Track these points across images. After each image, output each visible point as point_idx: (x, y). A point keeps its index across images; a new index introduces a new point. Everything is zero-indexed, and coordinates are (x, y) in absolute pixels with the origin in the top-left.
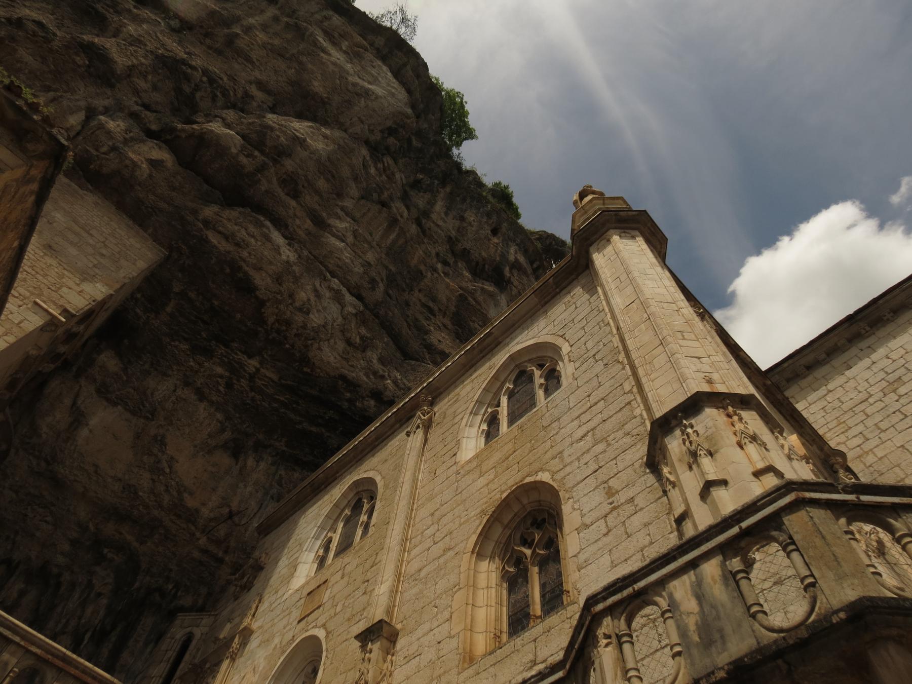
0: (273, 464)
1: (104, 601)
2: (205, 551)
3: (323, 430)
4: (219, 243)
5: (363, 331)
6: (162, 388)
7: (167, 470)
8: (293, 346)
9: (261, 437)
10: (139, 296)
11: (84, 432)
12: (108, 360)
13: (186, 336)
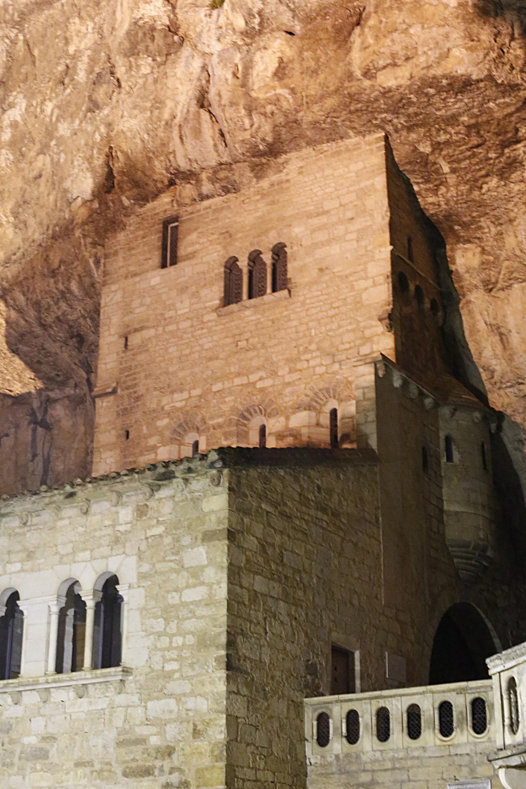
4: (396, 78)
11: (515, 339)
13: (483, 172)
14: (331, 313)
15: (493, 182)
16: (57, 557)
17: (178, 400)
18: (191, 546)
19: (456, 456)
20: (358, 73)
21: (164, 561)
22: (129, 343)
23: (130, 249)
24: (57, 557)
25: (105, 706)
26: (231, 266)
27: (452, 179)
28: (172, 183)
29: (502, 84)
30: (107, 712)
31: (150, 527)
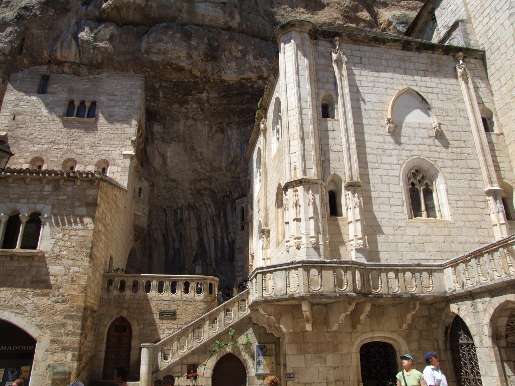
0: (238, 128)
1: (212, 205)
2: (232, 177)
3: (248, 105)
5: (240, 48)
6: (181, 127)
7: (202, 158)
8: (214, 79)
9: (227, 120)
10: (148, 98)
11: (169, 160)
12: (157, 128)
14: (111, 132)
15: (176, 106)
16: (8, 199)
17: (36, 147)
18: (80, 206)
19: (142, 195)
20: (143, 51)
21: (65, 209)
22: (16, 119)
23: (23, 81)
24: (8, 199)
25: (27, 265)
26: (72, 103)
27: (162, 100)
28: (49, 62)
29: (194, 74)
30: (27, 268)
31: (60, 196)
